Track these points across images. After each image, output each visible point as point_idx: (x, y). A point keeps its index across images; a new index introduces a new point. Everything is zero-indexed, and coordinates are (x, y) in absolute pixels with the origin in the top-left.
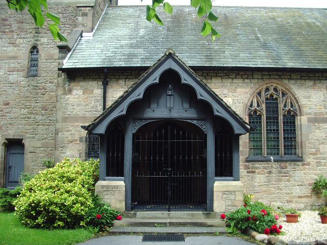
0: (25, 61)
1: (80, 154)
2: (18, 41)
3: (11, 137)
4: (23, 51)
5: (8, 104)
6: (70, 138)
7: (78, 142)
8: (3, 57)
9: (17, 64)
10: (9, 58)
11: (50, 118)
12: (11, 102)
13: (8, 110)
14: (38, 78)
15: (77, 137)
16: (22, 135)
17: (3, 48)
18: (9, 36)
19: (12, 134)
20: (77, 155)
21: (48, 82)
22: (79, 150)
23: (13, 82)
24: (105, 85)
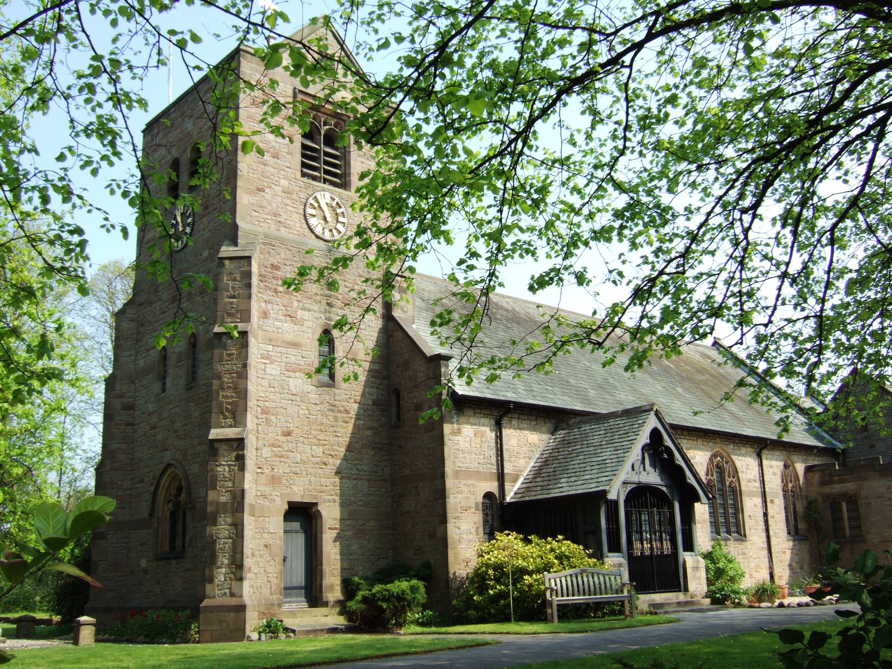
0: (312, 355)
1: (477, 528)
2: (300, 314)
3: (298, 499)
4: (310, 335)
5: (289, 434)
6: (463, 504)
7: (473, 510)
8: (276, 341)
9: (300, 358)
10: (287, 343)
11: (359, 467)
12: (296, 431)
13: (290, 445)
14: (337, 391)
15: (472, 503)
16: (316, 497)
17: (276, 323)
18: (285, 301)
19: (299, 495)
20: (473, 530)
21: (352, 400)
22: (475, 523)
23: (294, 391)
24: (498, 427)
